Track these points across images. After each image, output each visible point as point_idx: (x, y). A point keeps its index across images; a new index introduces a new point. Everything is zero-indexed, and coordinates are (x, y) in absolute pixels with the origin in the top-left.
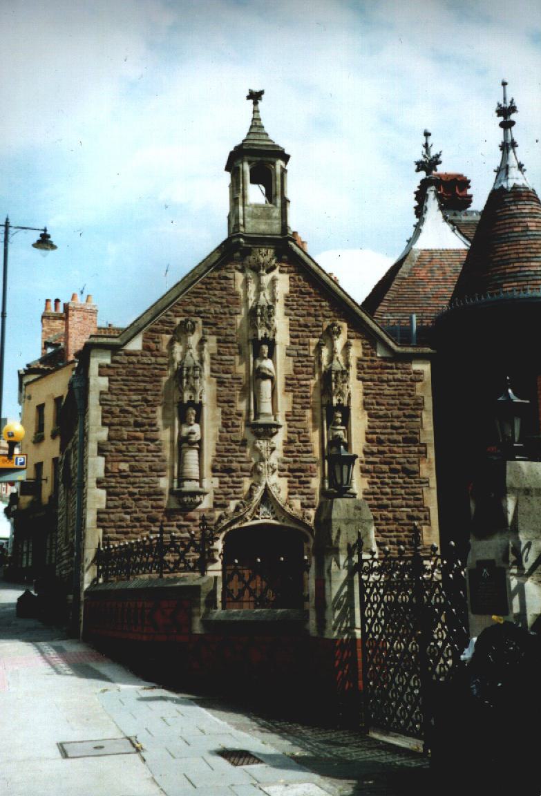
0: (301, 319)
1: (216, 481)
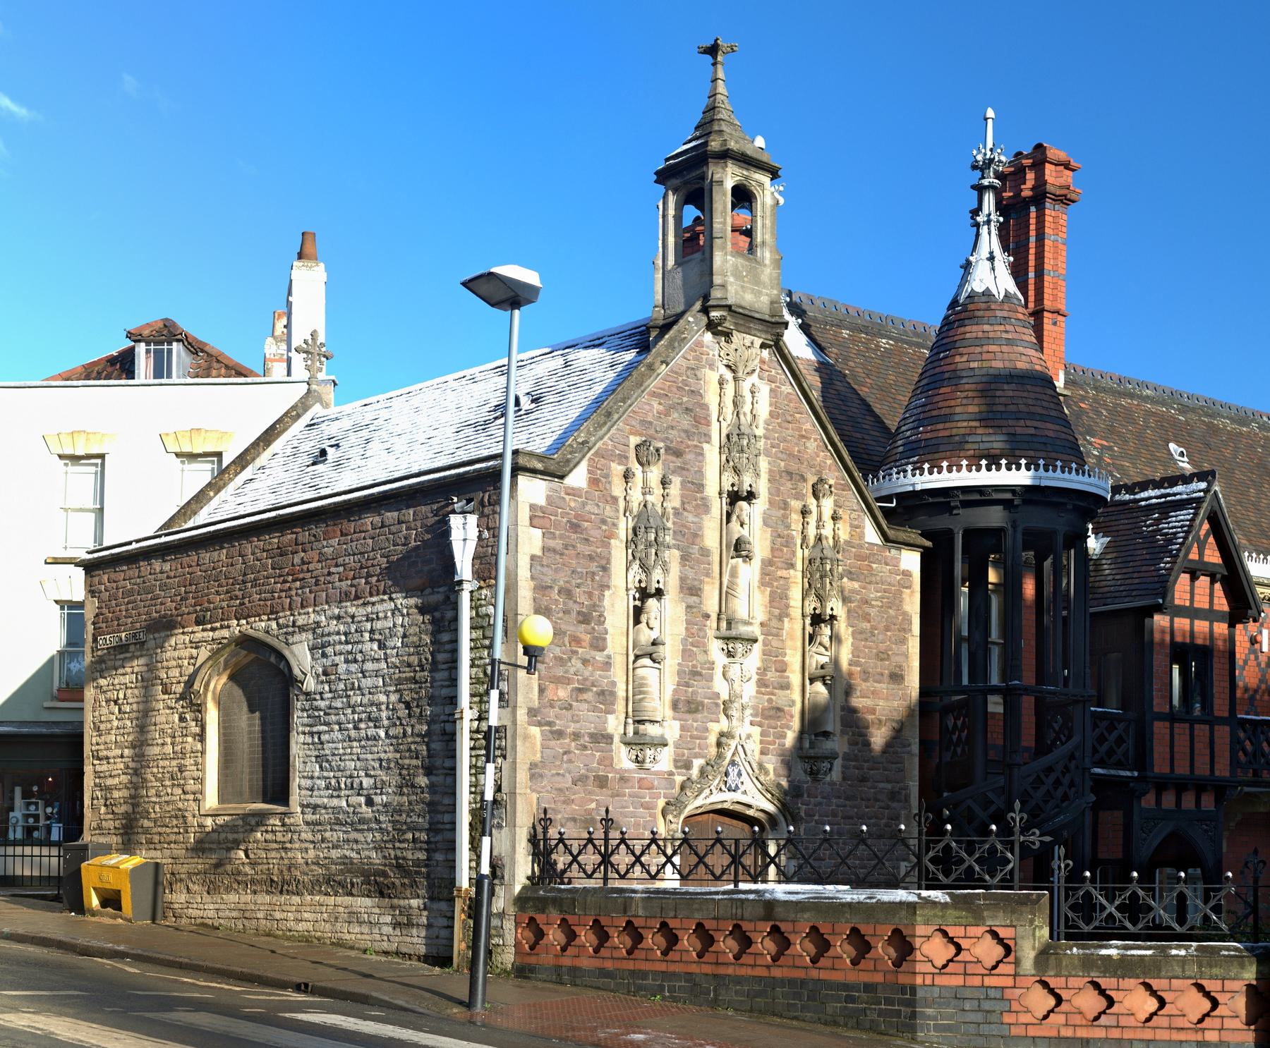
1: (677, 724)
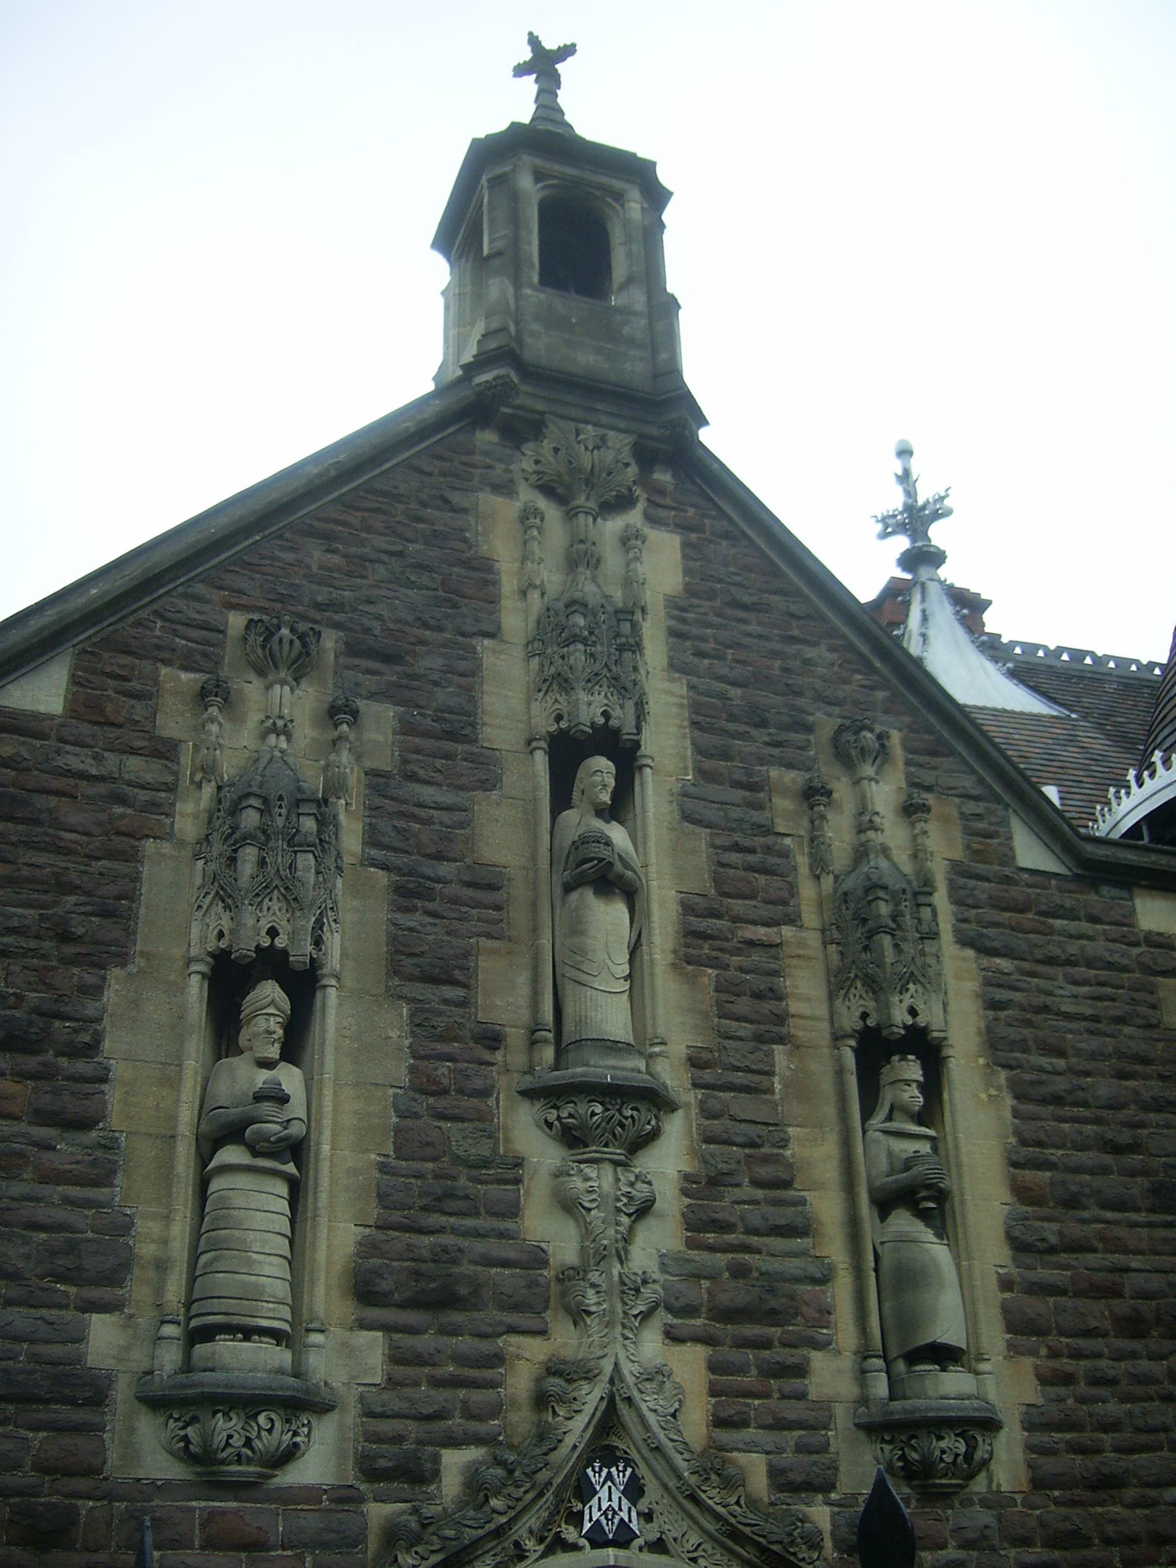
0: (735, 692)
